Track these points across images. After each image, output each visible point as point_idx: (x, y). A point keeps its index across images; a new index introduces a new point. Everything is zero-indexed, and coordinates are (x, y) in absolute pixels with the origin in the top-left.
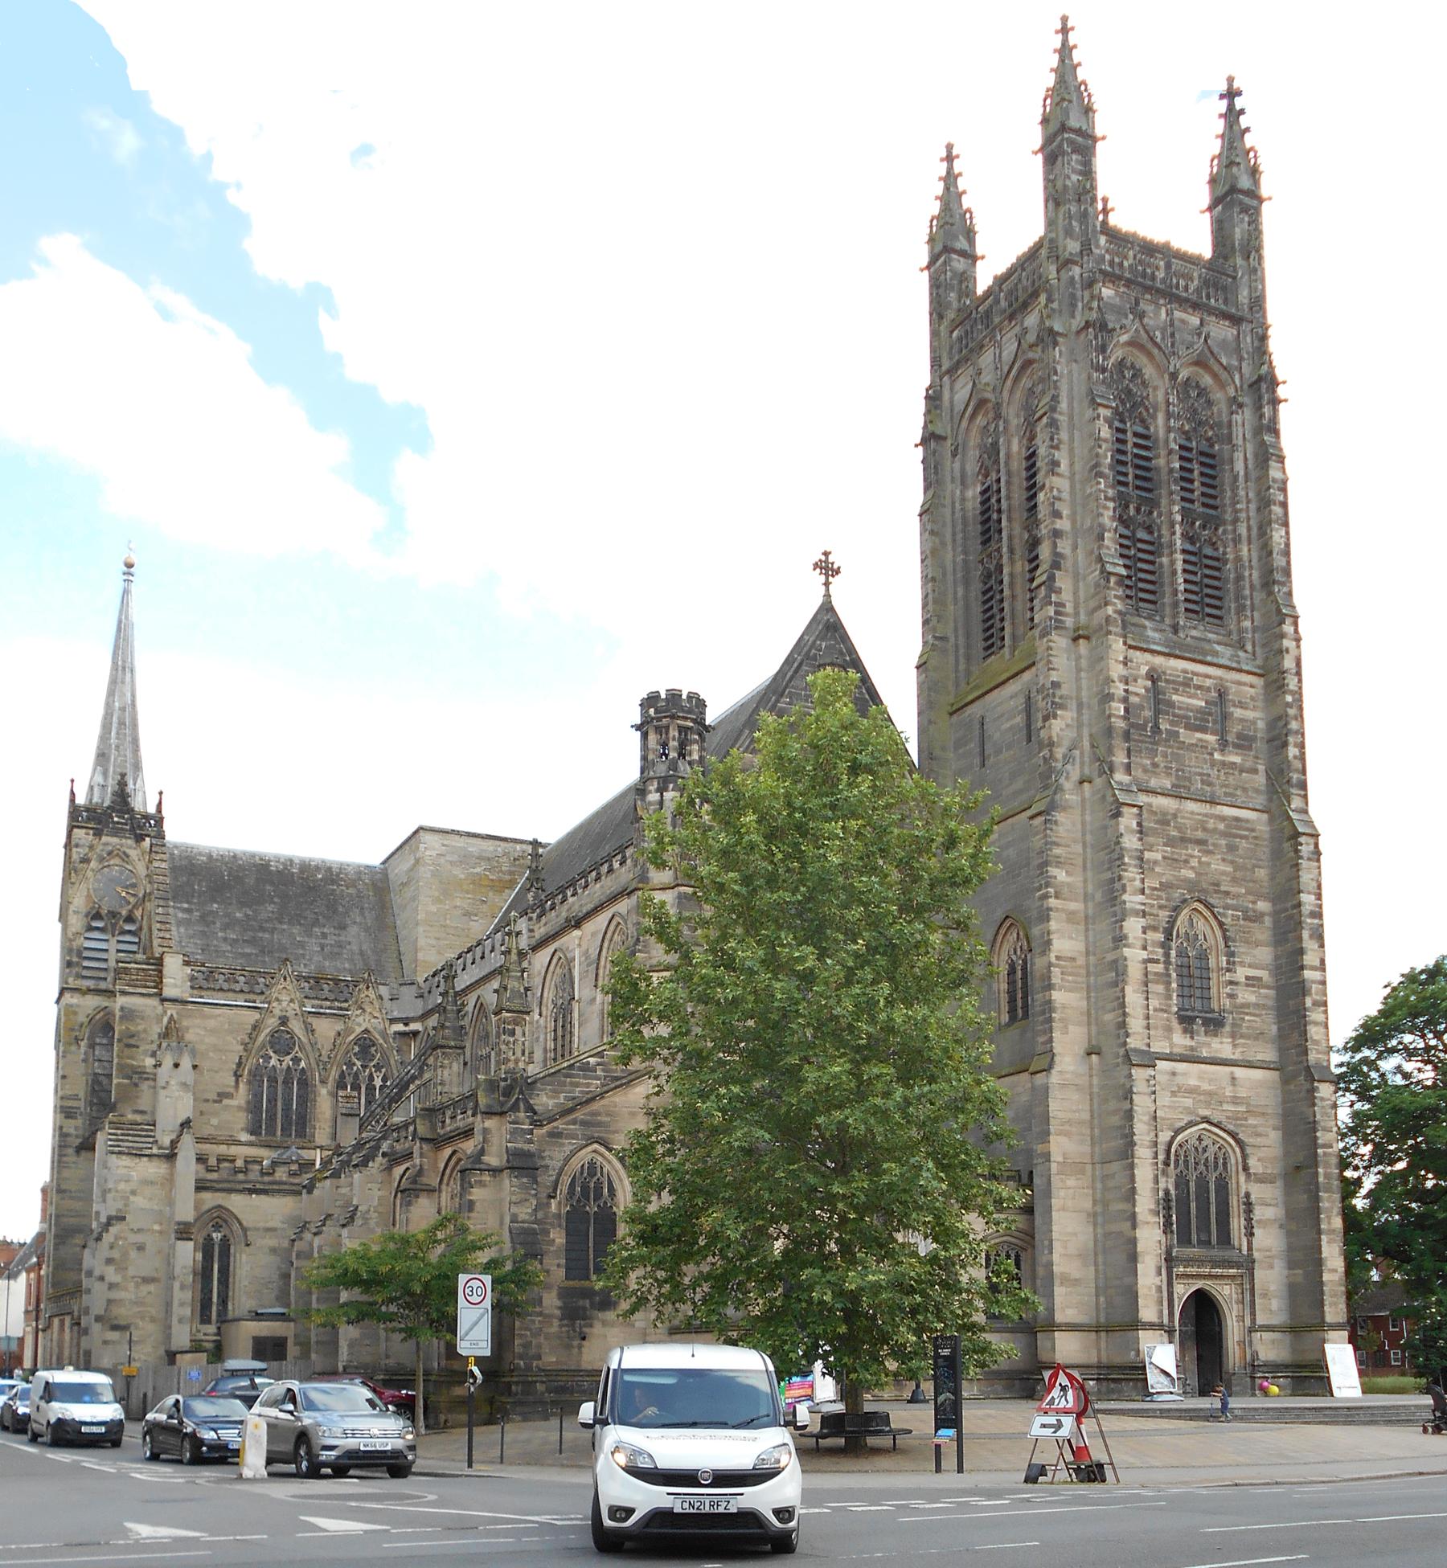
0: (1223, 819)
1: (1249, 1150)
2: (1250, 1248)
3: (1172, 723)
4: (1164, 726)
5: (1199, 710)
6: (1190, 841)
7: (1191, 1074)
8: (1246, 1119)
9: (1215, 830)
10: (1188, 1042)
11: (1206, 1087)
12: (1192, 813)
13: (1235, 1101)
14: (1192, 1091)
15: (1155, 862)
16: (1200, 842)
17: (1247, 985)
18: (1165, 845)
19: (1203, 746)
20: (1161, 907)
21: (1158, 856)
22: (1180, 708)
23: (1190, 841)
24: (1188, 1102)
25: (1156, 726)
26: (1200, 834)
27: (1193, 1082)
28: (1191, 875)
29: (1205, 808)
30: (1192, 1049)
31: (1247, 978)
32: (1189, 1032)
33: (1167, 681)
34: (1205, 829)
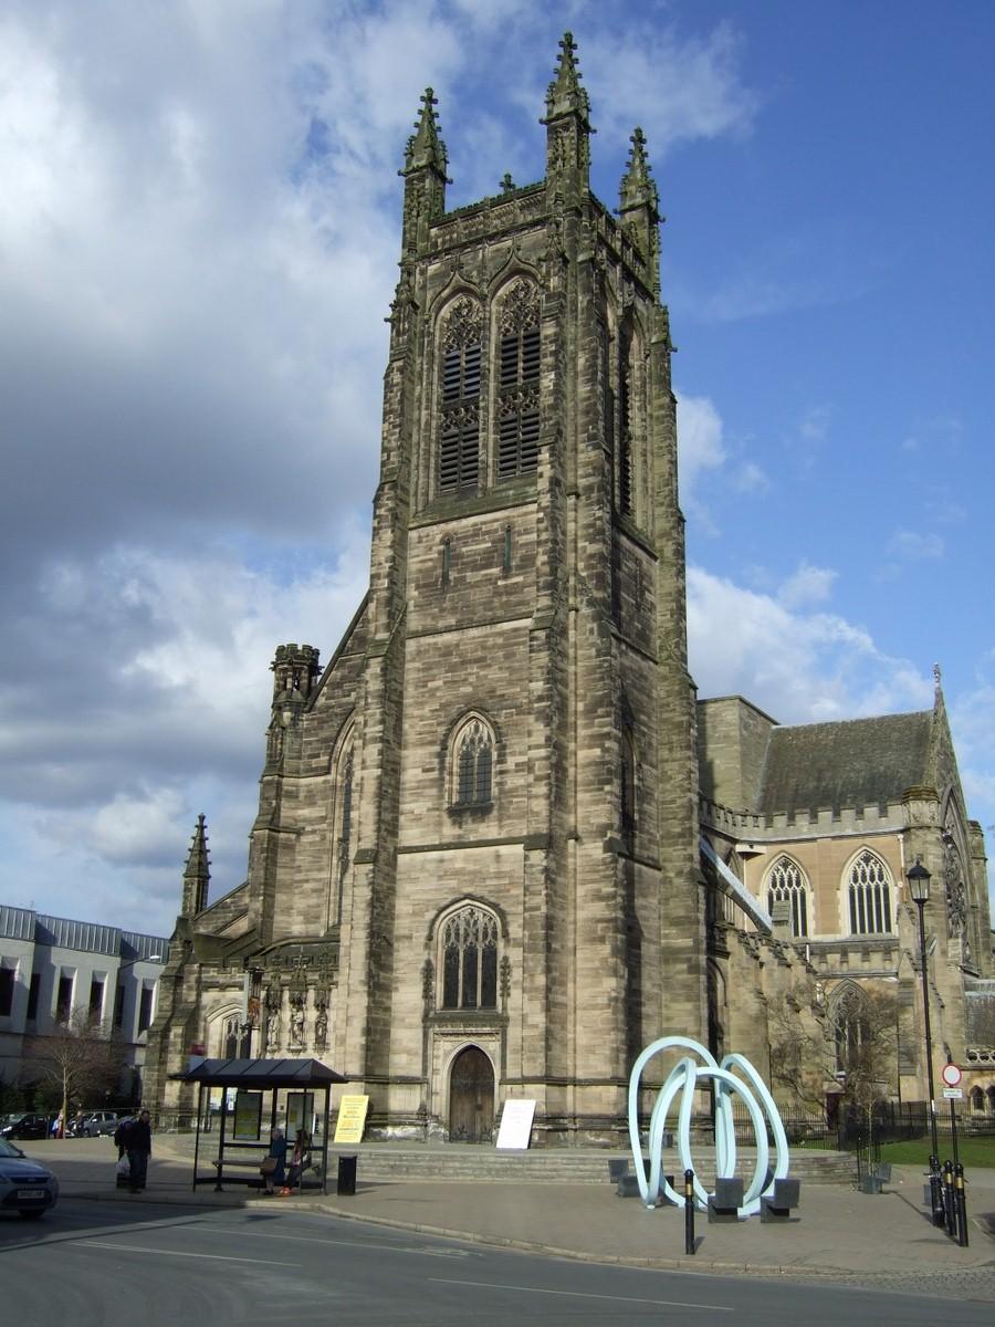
0: (500, 634)
1: (509, 918)
2: (504, 1008)
3: (459, 571)
4: (453, 575)
5: (487, 551)
6: (470, 662)
8: (508, 891)
9: (494, 646)
10: (457, 831)
11: (471, 867)
12: (474, 638)
13: (499, 875)
14: (458, 873)
15: (437, 689)
16: (477, 661)
17: (517, 771)
18: (447, 672)
19: (490, 580)
20: (438, 724)
21: (440, 683)
22: (468, 556)
23: (470, 662)
24: (453, 883)
25: (445, 577)
26: (480, 654)
27: (459, 865)
28: (469, 689)
29: (487, 630)
30: (460, 836)
31: (517, 765)
32: (458, 823)
33: (458, 539)
34: (484, 648)
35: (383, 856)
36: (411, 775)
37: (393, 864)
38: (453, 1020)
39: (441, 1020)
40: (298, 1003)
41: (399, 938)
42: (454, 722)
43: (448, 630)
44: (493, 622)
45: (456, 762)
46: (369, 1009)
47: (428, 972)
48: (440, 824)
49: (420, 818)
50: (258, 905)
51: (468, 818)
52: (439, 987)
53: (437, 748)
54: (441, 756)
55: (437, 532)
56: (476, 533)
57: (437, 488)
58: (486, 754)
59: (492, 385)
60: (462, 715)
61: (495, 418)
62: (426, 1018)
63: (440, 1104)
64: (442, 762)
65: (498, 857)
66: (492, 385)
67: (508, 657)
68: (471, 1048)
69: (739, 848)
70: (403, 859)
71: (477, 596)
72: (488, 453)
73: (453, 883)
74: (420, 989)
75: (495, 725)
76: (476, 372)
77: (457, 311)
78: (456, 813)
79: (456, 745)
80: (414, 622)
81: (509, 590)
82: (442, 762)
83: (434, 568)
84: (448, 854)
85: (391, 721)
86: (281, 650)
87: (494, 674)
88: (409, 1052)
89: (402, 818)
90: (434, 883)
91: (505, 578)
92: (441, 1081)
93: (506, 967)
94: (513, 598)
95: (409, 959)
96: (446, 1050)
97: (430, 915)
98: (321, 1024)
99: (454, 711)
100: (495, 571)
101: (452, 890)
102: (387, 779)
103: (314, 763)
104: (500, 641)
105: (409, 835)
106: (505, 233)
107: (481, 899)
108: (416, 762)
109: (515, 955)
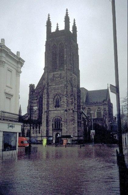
4: (54, 79)
36: (50, 102)
40: (36, 128)
49: (52, 107)
50: (29, 116)
52: (54, 126)
54: (54, 100)
55: (52, 74)
69: (83, 107)
74: (52, 126)
78: (55, 107)
79: (55, 99)
80: (50, 84)
86: (30, 85)
93: (62, 124)
95: (51, 123)
98: (39, 130)
103: (35, 99)
105: (50, 109)
108: (51, 100)
109: (63, 123)
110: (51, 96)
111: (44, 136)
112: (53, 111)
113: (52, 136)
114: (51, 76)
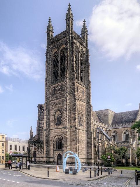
0: (61, 100)
7: (57, 130)
11: (58, 131)
14: (57, 132)
19: (60, 93)
24: (56, 133)
25: (54, 93)
27: (57, 131)
28: (58, 108)
32: (57, 126)
35: (47, 130)
36: (51, 120)
37: (49, 131)
38: (57, 150)
39: (56, 150)
41: (50, 141)
42: (56, 112)
43: (55, 100)
44: (60, 98)
45: (56, 118)
46: (46, 149)
47: (54, 145)
48: (54, 126)
49: (52, 126)
51: (58, 125)
52: (55, 146)
53: (54, 116)
54: (54, 117)
55: (53, 86)
56: (58, 86)
57: (53, 80)
58: (60, 117)
59: (60, 64)
60: (57, 111)
61: (60, 69)
62: (54, 150)
63: (56, 160)
64: (55, 118)
65: (62, 130)
66: (60, 64)
67: (62, 103)
68: (60, 154)
70: (50, 131)
71: (58, 95)
72: (59, 75)
73: (56, 133)
74: (53, 147)
75: (61, 113)
76: (57, 62)
77: (55, 53)
78: (56, 125)
79: (56, 115)
80: (51, 99)
81: (62, 94)
82: (55, 118)
83: (53, 92)
84: (56, 130)
85: (48, 113)
87: (61, 106)
88: (52, 154)
89: (50, 126)
90: (54, 134)
91: (62, 92)
92: (56, 158)
94: (63, 95)
95: (52, 143)
96: (57, 154)
97: (54, 138)
99: (56, 111)
100: (60, 91)
101: (56, 134)
102: (47, 120)
104: (61, 101)
105: (51, 127)
106: (61, 39)
107: (60, 135)
108: (52, 118)
110: (52, 112)
111: (44, 157)
112: (54, 130)
113: (53, 156)
114: (51, 90)
